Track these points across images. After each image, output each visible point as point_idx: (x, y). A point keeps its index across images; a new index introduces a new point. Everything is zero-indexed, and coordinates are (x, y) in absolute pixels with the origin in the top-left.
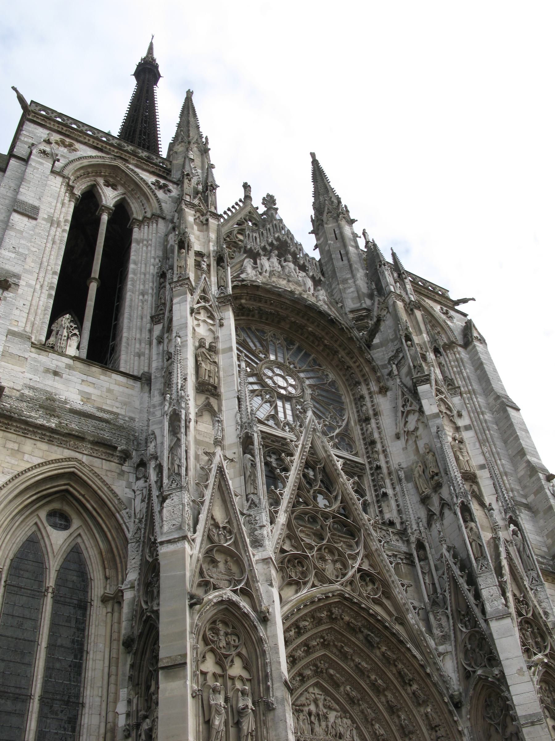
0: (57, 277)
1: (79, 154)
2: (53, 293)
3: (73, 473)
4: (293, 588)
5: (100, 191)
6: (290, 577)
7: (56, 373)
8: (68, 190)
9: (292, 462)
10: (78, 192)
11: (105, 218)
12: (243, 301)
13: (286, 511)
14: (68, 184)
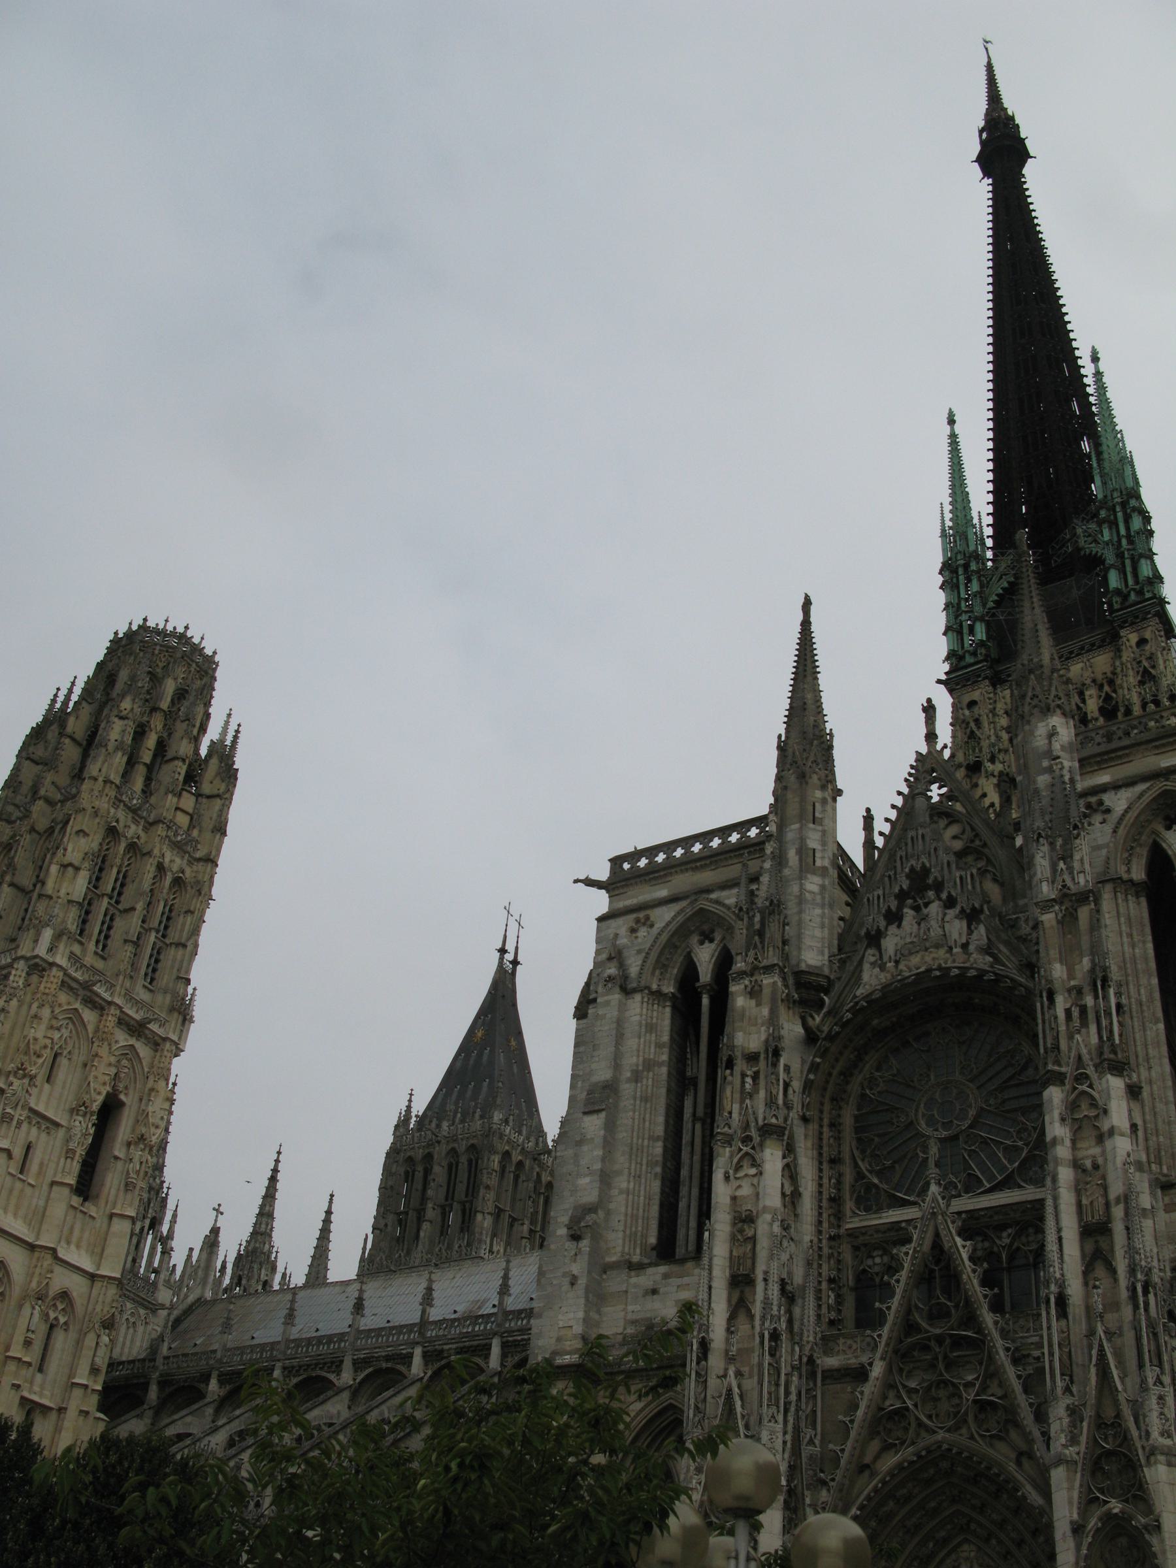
0: (660, 1144)
1: (659, 925)
2: (658, 1169)
3: (671, 1404)
4: (894, 1450)
5: (695, 959)
6: (886, 1441)
7: (654, 1292)
8: (654, 1000)
9: (898, 1281)
10: (669, 988)
11: (705, 1001)
12: (875, 1022)
13: (882, 1359)
14: (652, 993)
